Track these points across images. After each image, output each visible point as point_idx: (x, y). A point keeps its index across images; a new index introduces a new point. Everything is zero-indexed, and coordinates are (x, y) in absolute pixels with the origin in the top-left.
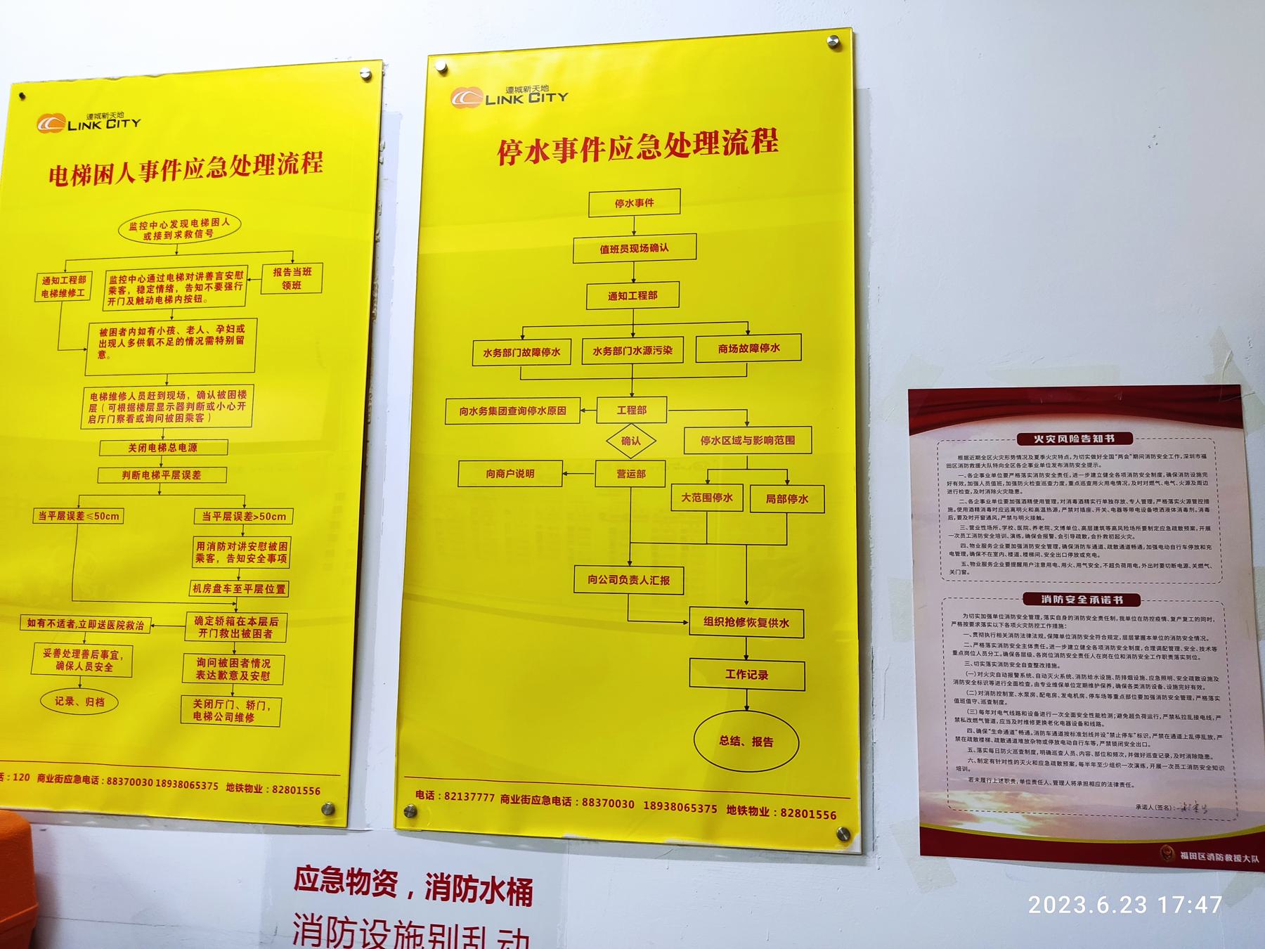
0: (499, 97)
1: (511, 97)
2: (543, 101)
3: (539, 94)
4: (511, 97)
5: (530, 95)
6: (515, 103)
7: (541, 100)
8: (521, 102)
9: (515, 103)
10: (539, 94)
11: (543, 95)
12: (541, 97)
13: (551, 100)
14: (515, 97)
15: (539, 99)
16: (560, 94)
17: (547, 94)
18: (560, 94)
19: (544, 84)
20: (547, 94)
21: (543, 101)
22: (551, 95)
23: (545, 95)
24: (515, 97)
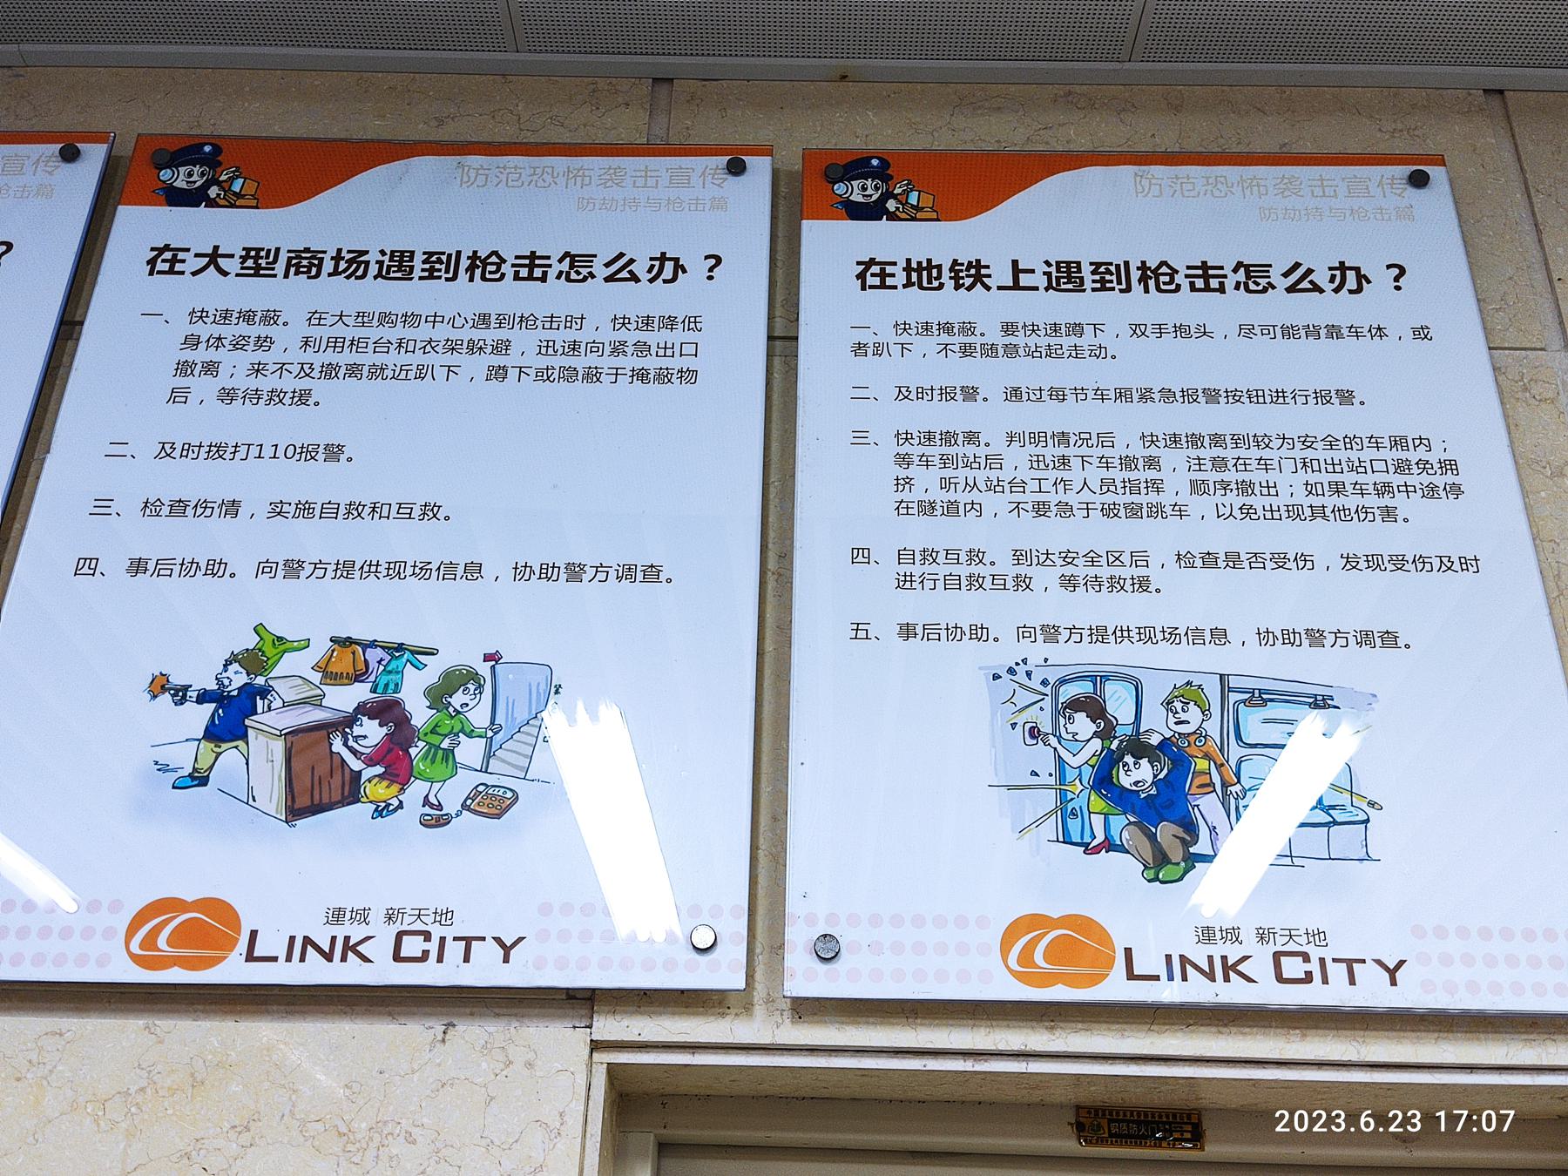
0: (292, 939)
1: (334, 939)
2: (440, 959)
3: (427, 936)
4: (334, 939)
5: (400, 936)
6: (344, 959)
7: (433, 955)
8: (366, 959)
9: (344, 959)
10: (427, 936)
11: (443, 939)
12: (433, 947)
13: (466, 959)
14: (347, 939)
15: (426, 954)
16: (498, 940)
17: (455, 939)
18: (498, 940)
19: (442, 907)
20: (455, 939)
21: (440, 959)
22: (469, 941)
23: (449, 942)
24: (347, 939)
